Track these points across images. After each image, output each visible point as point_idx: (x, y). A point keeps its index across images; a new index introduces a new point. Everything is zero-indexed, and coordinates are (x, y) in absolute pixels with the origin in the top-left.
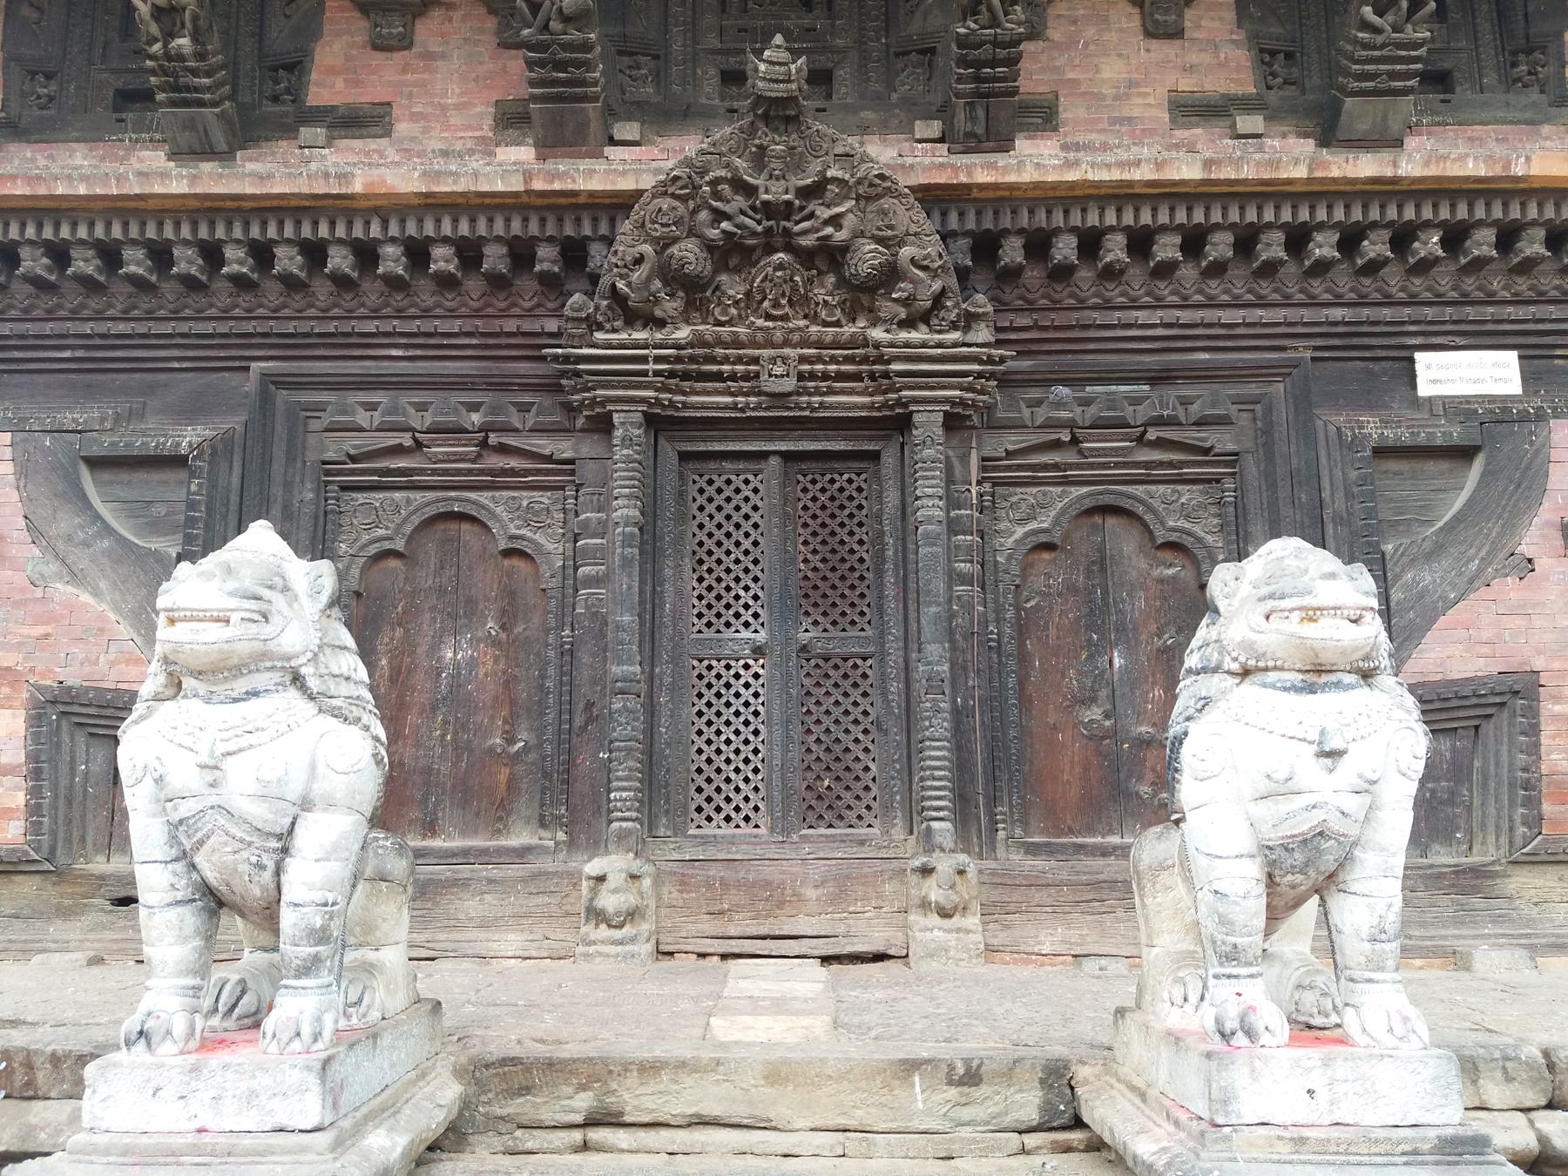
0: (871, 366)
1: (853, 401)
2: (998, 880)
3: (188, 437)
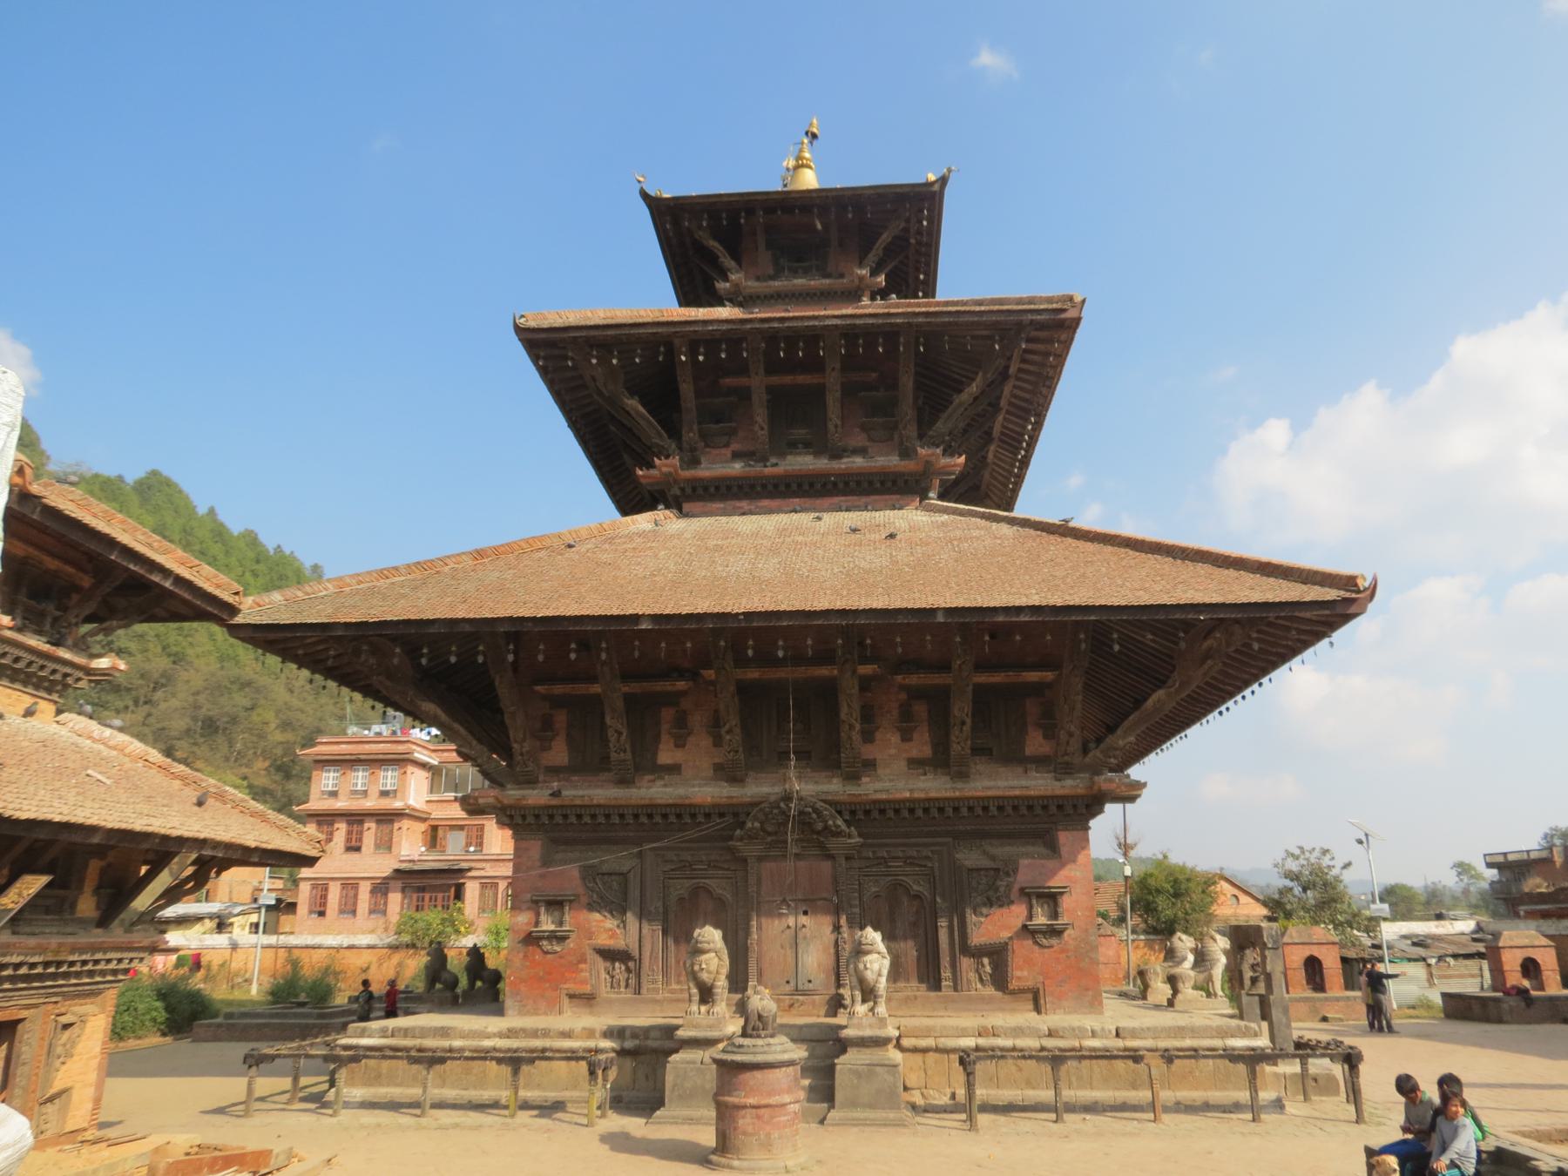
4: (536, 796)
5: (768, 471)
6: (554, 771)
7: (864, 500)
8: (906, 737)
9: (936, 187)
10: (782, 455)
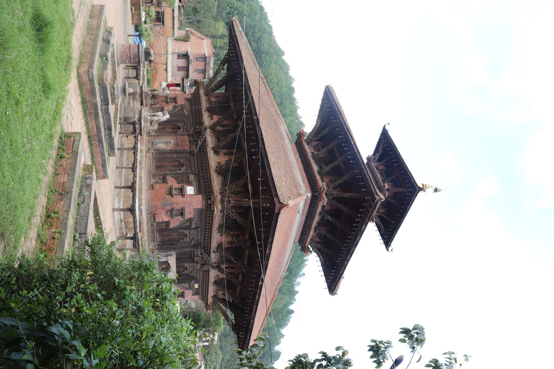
4: (202, 92)
6: (209, 99)
7: (307, 182)
9: (418, 189)
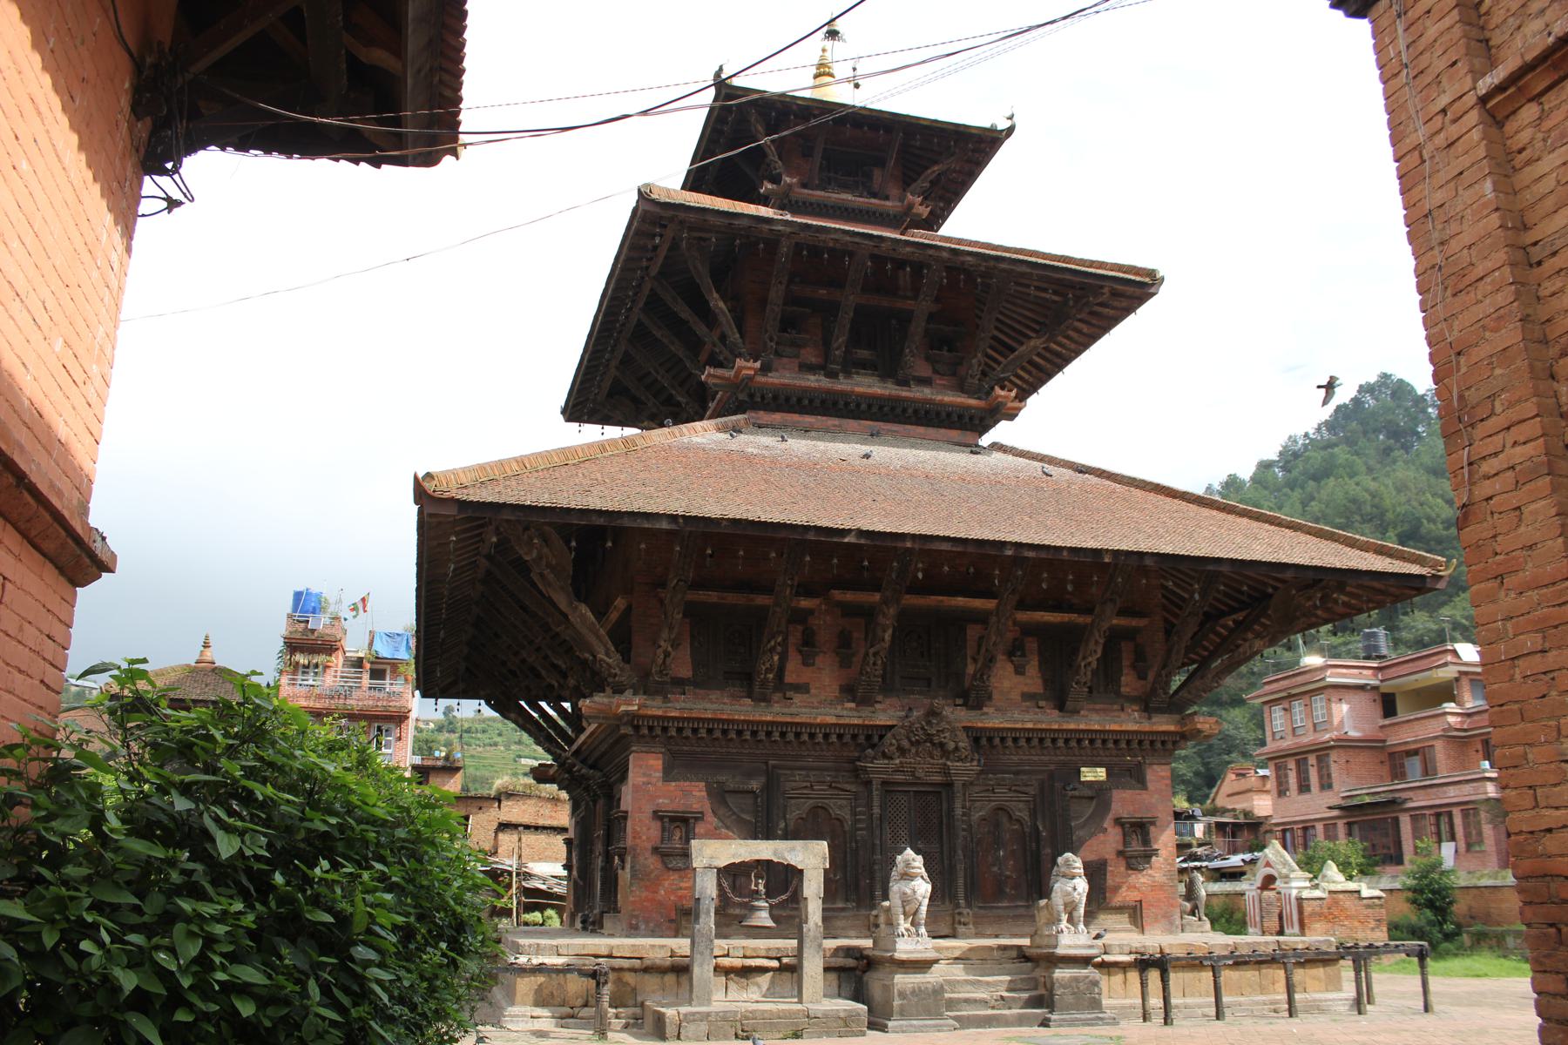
0: (945, 771)
1: (938, 778)
2: (975, 916)
3: (755, 785)
5: (839, 387)
6: (679, 683)
8: (1019, 670)
10: (848, 374)
